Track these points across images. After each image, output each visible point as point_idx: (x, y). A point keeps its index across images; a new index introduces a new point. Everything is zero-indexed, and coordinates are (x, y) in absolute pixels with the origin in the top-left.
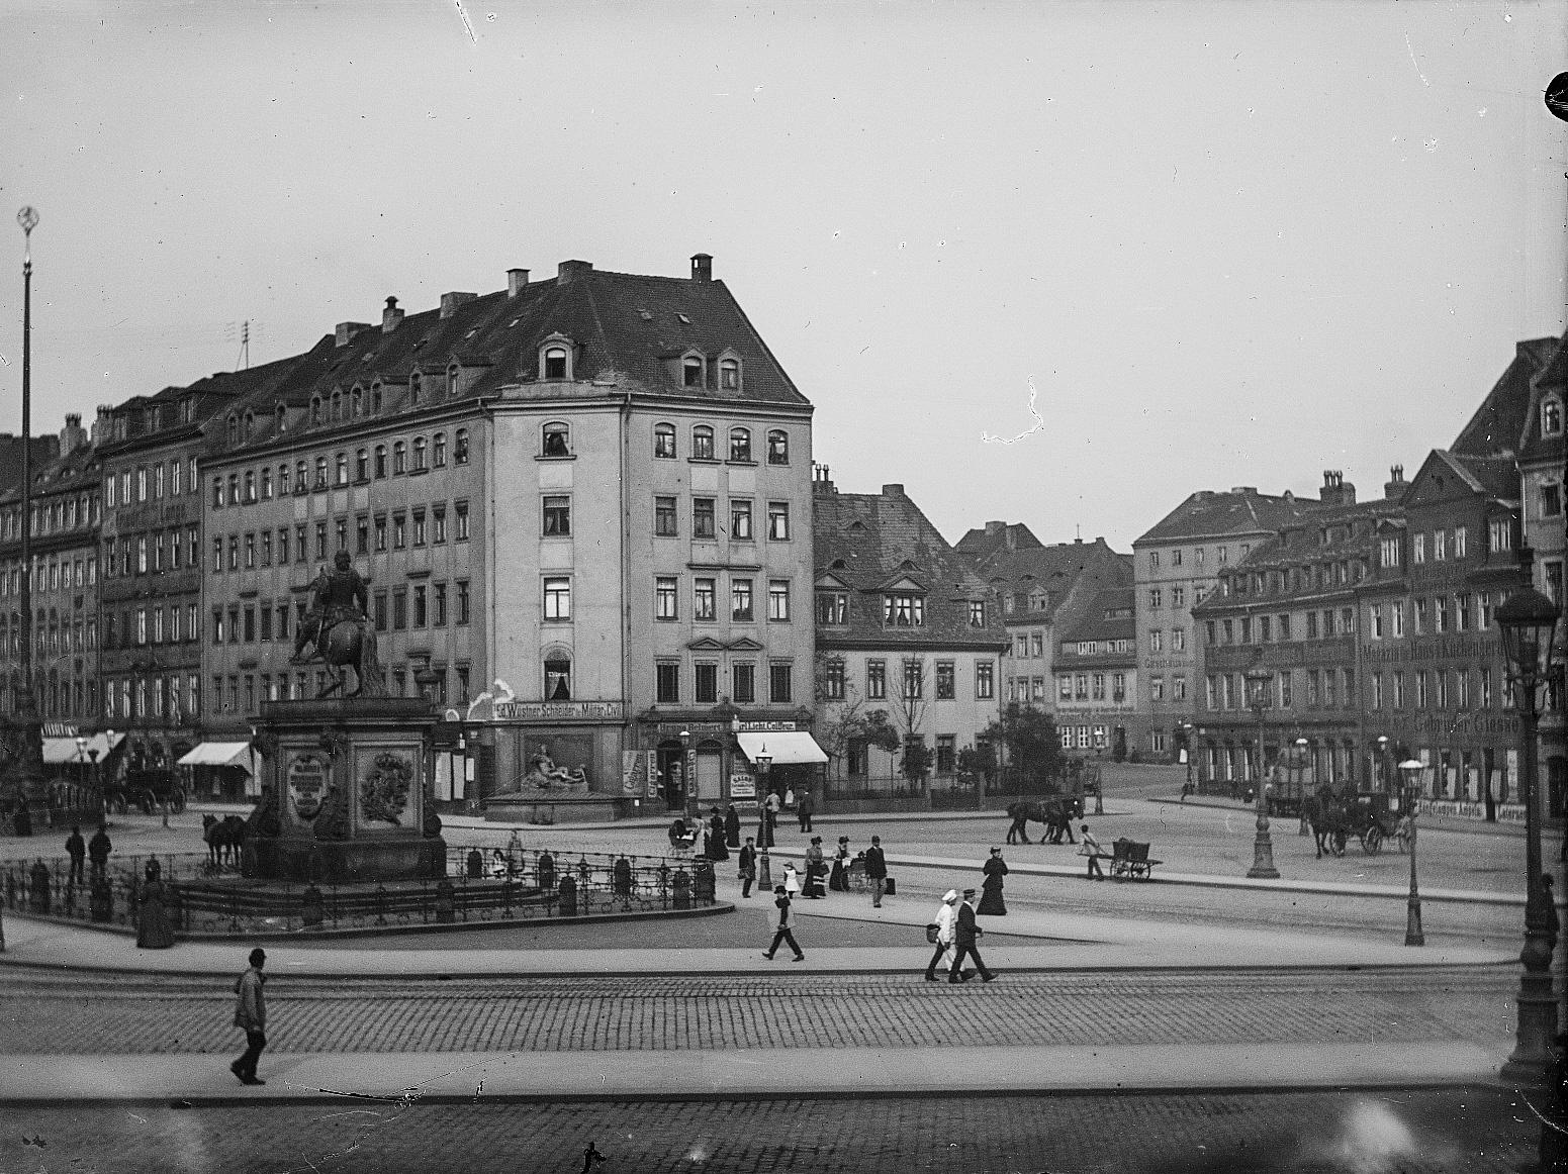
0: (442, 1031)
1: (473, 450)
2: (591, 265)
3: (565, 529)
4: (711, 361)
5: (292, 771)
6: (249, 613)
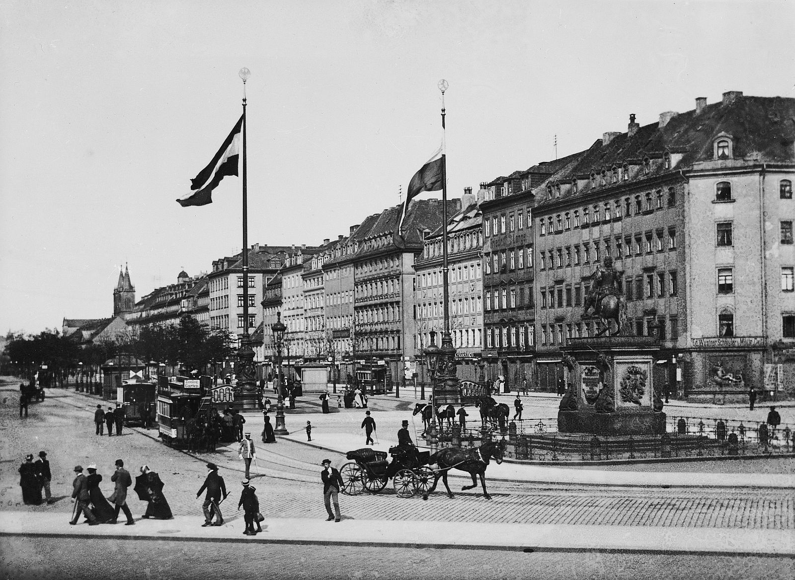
0: (610, 514)
2: (742, 93)
3: (729, 243)
5: (584, 376)
6: (560, 291)
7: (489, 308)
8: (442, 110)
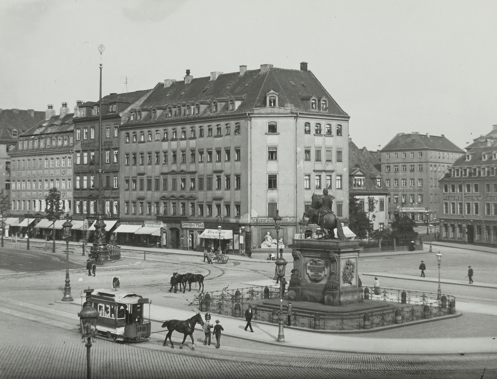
1: (242, 130)
2: (273, 65)
4: (319, 101)
6: (142, 180)
7: (78, 186)
8: (100, 65)
